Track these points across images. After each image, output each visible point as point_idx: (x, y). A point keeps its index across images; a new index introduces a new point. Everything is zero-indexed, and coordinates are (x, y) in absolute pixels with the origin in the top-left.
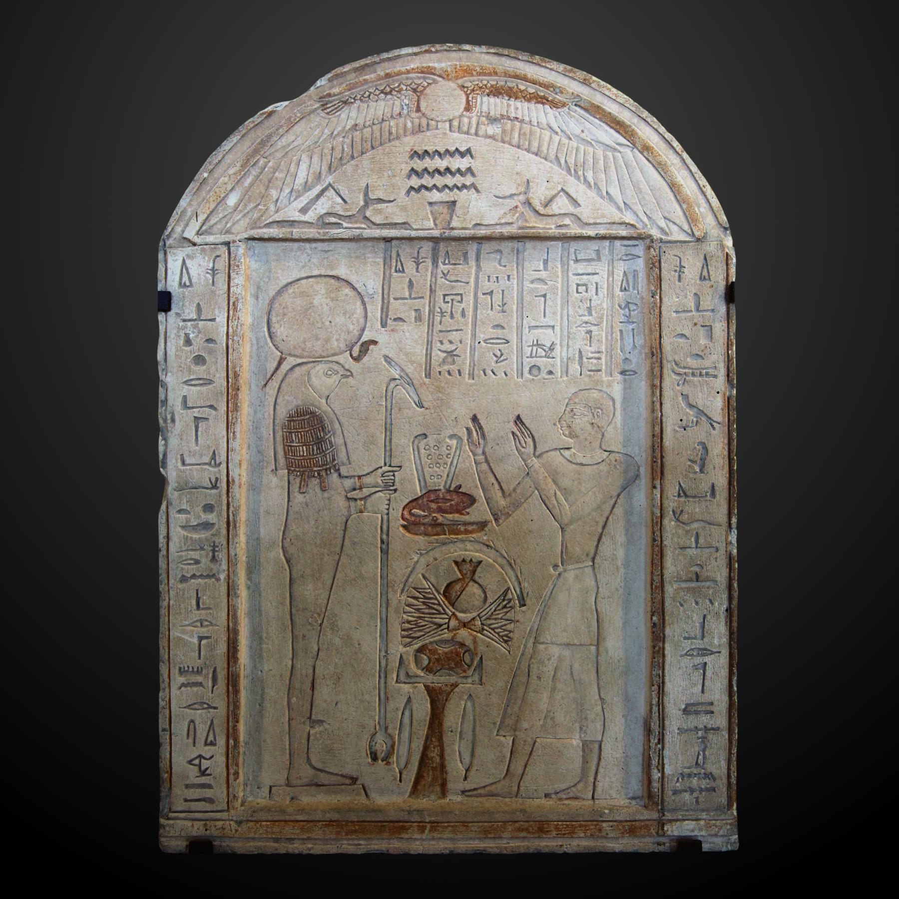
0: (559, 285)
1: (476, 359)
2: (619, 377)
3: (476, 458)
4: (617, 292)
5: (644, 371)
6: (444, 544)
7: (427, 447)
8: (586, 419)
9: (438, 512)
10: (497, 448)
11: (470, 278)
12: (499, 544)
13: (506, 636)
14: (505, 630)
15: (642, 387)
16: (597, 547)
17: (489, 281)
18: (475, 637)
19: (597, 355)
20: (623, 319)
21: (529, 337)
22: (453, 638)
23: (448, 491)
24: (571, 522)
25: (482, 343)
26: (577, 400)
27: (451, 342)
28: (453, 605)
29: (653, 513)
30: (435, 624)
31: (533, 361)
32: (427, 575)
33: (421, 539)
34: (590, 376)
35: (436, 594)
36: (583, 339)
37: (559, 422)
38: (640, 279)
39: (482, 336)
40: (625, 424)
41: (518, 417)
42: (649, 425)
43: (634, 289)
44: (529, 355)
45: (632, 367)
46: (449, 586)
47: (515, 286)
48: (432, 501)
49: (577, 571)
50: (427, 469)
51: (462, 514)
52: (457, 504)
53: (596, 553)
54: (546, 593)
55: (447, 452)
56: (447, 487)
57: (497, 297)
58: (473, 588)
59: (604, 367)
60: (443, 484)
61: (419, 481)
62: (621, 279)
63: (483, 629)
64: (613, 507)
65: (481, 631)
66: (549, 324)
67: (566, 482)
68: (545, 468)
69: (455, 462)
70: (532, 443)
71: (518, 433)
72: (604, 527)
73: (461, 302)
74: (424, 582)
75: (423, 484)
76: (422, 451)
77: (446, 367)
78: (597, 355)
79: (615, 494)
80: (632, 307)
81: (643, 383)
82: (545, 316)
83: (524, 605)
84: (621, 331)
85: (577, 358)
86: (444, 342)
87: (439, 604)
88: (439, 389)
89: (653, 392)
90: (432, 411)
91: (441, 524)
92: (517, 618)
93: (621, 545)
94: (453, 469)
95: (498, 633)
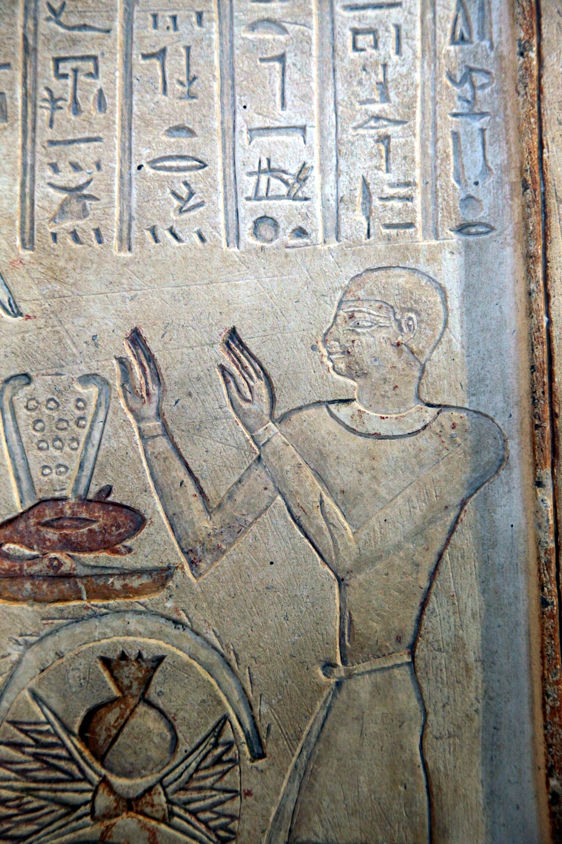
0: (314, 34)
1: (134, 205)
2: (455, 239)
3: (143, 425)
4: (446, 47)
5: (508, 224)
6: (78, 620)
7: (32, 404)
8: (383, 334)
9: (61, 550)
10: (186, 401)
11: (112, 19)
12: (200, 618)
13: (224, 827)
14: (220, 815)
15: (506, 260)
16: (419, 620)
17: (155, 26)
18: (153, 833)
19: (403, 191)
20: (460, 107)
21: (251, 153)
22: (104, 834)
23: (84, 501)
24: (360, 564)
25: (146, 168)
26: (361, 293)
27: (76, 167)
28: (101, 758)
29: (539, 543)
30: (63, 804)
31: (262, 207)
32: (41, 693)
33: (25, 611)
34: (389, 238)
35: (64, 736)
36: (372, 156)
37: (325, 341)
38: (495, 15)
39: (145, 152)
40: (470, 344)
41: (233, 332)
42: (524, 346)
43: (482, 38)
44: (250, 193)
45: (482, 215)
46: (92, 716)
47: (215, 37)
48: (47, 524)
49: (378, 677)
50: (33, 455)
51: (117, 552)
52: (104, 530)
53: (417, 634)
54: (310, 726)
55: (78, 413)
56: (81, 491)
57: (176, 64)
58: (146, 720)
59: (419, 218)
60: (70, 485)
61: (18, 479)
62: (452, 14)
63: (172, 814)
64: (452, 531)
65: (167, 819)
66: (294, 123)
67: (343, 476)
68: (297, 446)
69: (96, 435)
70: (264, 392)
71: (234, 369)
72: (433, 576)
73: (94, 75)
74: (36, 708)
75: (25, 485)
76: (22, 413)
77: (68, 224)
78: (403, 191)
79: (455, 500)
80: (479, 79)
81: (509, 250)
82: (283, 105)
83: (262, 756)
84: (456, 135)
85: (359, 200)
86: (61, 166)
87: (71, 759)
88: (55, 275)
89: (528, 271)
90: (41, 322)
91: (68, 576)
92: (246, 786)
93: (473, 615)
94: (92, 452)
95: (205, 823)
